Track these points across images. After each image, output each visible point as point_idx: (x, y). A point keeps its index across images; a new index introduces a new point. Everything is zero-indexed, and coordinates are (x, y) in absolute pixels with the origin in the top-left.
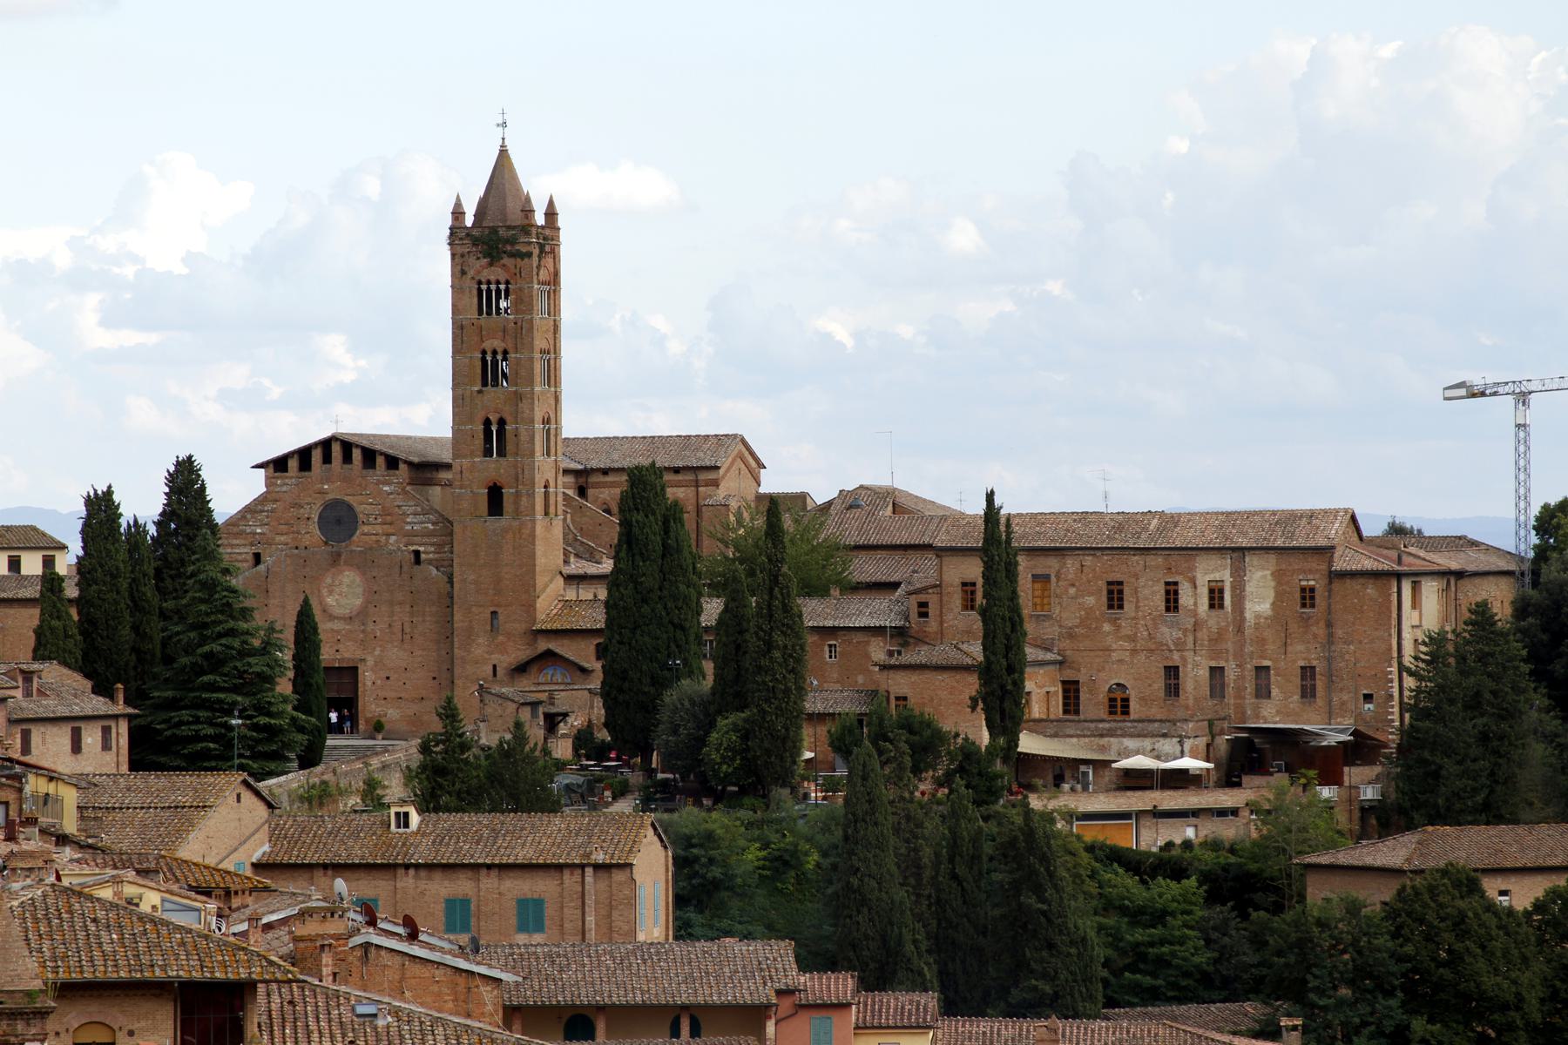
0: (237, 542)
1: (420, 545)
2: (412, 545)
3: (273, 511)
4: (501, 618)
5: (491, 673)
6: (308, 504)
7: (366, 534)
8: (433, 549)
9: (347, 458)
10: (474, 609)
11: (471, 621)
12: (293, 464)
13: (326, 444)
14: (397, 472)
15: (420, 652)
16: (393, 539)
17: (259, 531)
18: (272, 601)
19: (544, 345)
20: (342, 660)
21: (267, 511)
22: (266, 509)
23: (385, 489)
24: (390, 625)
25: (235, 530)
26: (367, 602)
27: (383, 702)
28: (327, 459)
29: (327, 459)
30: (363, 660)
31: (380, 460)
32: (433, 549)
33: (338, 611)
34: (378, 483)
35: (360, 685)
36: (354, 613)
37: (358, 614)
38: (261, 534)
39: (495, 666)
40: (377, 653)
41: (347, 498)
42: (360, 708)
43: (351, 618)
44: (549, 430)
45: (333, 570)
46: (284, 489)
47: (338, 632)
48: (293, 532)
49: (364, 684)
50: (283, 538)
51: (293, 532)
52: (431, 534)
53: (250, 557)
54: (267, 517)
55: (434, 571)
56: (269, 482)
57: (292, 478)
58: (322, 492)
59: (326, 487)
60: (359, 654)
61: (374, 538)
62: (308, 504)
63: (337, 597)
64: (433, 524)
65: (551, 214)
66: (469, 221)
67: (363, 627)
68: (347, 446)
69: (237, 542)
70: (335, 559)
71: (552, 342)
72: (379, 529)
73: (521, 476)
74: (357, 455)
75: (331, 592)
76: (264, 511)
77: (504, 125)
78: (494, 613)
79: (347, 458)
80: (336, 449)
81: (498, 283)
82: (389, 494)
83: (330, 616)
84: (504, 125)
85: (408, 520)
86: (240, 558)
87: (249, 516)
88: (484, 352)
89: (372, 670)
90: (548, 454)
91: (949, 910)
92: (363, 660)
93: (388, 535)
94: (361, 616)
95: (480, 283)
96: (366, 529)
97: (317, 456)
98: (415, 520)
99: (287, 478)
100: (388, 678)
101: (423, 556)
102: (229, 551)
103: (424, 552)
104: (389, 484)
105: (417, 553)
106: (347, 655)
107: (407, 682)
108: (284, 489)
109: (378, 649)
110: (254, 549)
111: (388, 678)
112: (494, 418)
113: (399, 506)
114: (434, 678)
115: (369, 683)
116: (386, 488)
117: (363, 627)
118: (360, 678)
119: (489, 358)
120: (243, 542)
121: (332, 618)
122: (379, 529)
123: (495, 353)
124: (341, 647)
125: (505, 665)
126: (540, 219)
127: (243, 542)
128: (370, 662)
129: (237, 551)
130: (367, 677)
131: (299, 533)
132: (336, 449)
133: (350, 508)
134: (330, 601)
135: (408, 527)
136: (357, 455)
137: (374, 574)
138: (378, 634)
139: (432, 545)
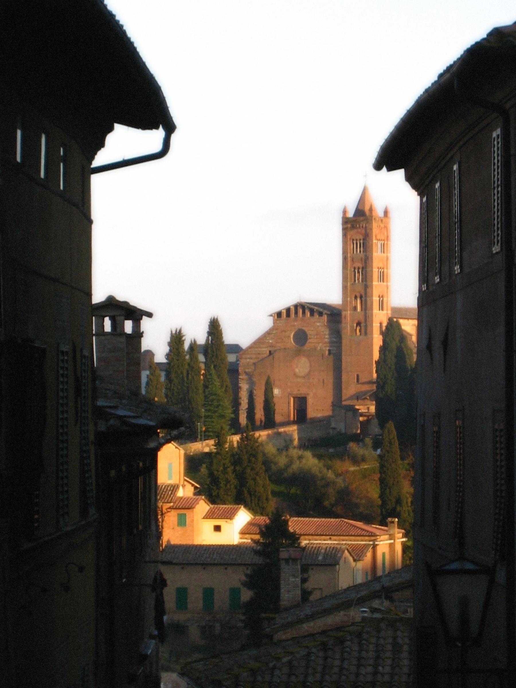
4: (360, 377)
7: (312, 342)
13: (296, 306)
17: (271, 341)
19: (381, 265)
20: (301, 394)
22: (273, 333)
23: (318, 324)
26: (310, 371)
28: (296, 313)
29: (296, 313)
30: (308, 394)
38: (271, 343)
40: (314, 391)
41: (304, 328)
44: (382, 301)
54: (274, 336)
56: (275, 322)
58: (294, 326)
61: (313, 344)
65: (386, 213)
66: (351, 214)
70: (298, 353)
71: (386, 264)
72: (315, 341)
75: (297, 367)
77: (366, 176)
78: (358, 376)
81: (360, 240)
84: (366, 176)
88: (355, 268)
90: (382, 310)
91: (253, 504)
93: (319, 343)
94: (307, 376)
95: (353, 240)
103: (333, 350)
104: (319, 322)
122: (315, 341)
123: (359, 268)
126: (381, 214)
128: (311, 394)
130: (310, 401)
134: (297, 370)
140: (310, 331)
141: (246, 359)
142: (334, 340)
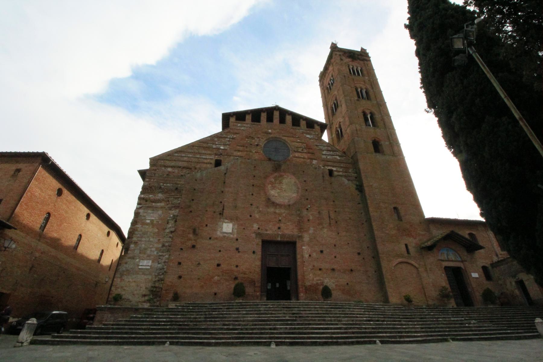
0: (206, 152)
1: (333, 166)
2: (328, 166)
3: (233, 139)
5: (406, 252)
6: (258, 138)
8: (341, 170)
9: (282, 121)
10: (381, 204)
11: (381, 212)
12: (249, 117)
14: (314, 130)
15: (344, 233)
16: (314, 162)
17: (222, 148)
18: (227, 189)
21: (230, 138)
22: (229, 137)
23: (308, 136)
24: (319, 212)
25: (205, 145)
27: (319, 272)
29: (270, 119)
31: (303, 123)
32: (341, 170)
33: (279, 201)
34: (303, 133)
35: (298, 256)
36: (291, 202)
37: (295, 204)
39: (406, 245)
40: (311, 231)
41: (284, 138)
42: (299, 277)
43: (289, 205)
45: (276, 174)
46: (243, 128)
47: (280, 214)
48: (247, 151)
49: (303, 256)
50: (239, 154)
51: (247, 151)
52: (340, 162)
53: (213, 162)
54: (229, 141)
55: (346, 182)
57: (248, 124)
59: (270, 131)
60: (296, 232)
61: (302, 160)
62: (258, 138)
63: (278, 191)
64: (339, 156)
67: (298, 212)
68: (283, 113)
69: (203, 152)
70: (277, 168)
73: (390, 137)
74: (289, 118)
75: (274, 188)
76: (227, 138)
79: (282, 121)
80: (276, 114)
82: (310, 139)
83: (273, 203)
85: (324, 153)
86: (206, 161)
87: (216, 139)
89: (309, 245)
92: (301, 237)
93: (312, 159)
96: (297, 155)
97: (264, 116)
98: (328, 154)
99: (245, 124)
100: (322, 252)
101: (336, 173)
102: (198, 156)
105: (331, 173)
106: (287, 232)
107: (338, 256)
108: (243, 128)
109: (312, 229)
110: (217, 157)
111: (322, 252)
112: (368, 112)
113: (317, 145)
114: (359, 254)
115: (307, 256)
116: (308, 136)
117: (298, 212)
118: (298, 251)
119: (359, 90)
120: (209, 152)
121: (274, 204)
124: (282, 225)
125: (414, 245)
127: (209, 152)
128: (306, 237)
129: (204, 157)
131: (251, 152)
132: (276, 114)
133: (285, 143)
134: (273, 193)
135: (324, 157)
136: (289, 118)
137: (305, 179)
138: (311, 218)
139: (342, 167)
140: (293, 143)
141: (166, 167)
142: (338, 158)
